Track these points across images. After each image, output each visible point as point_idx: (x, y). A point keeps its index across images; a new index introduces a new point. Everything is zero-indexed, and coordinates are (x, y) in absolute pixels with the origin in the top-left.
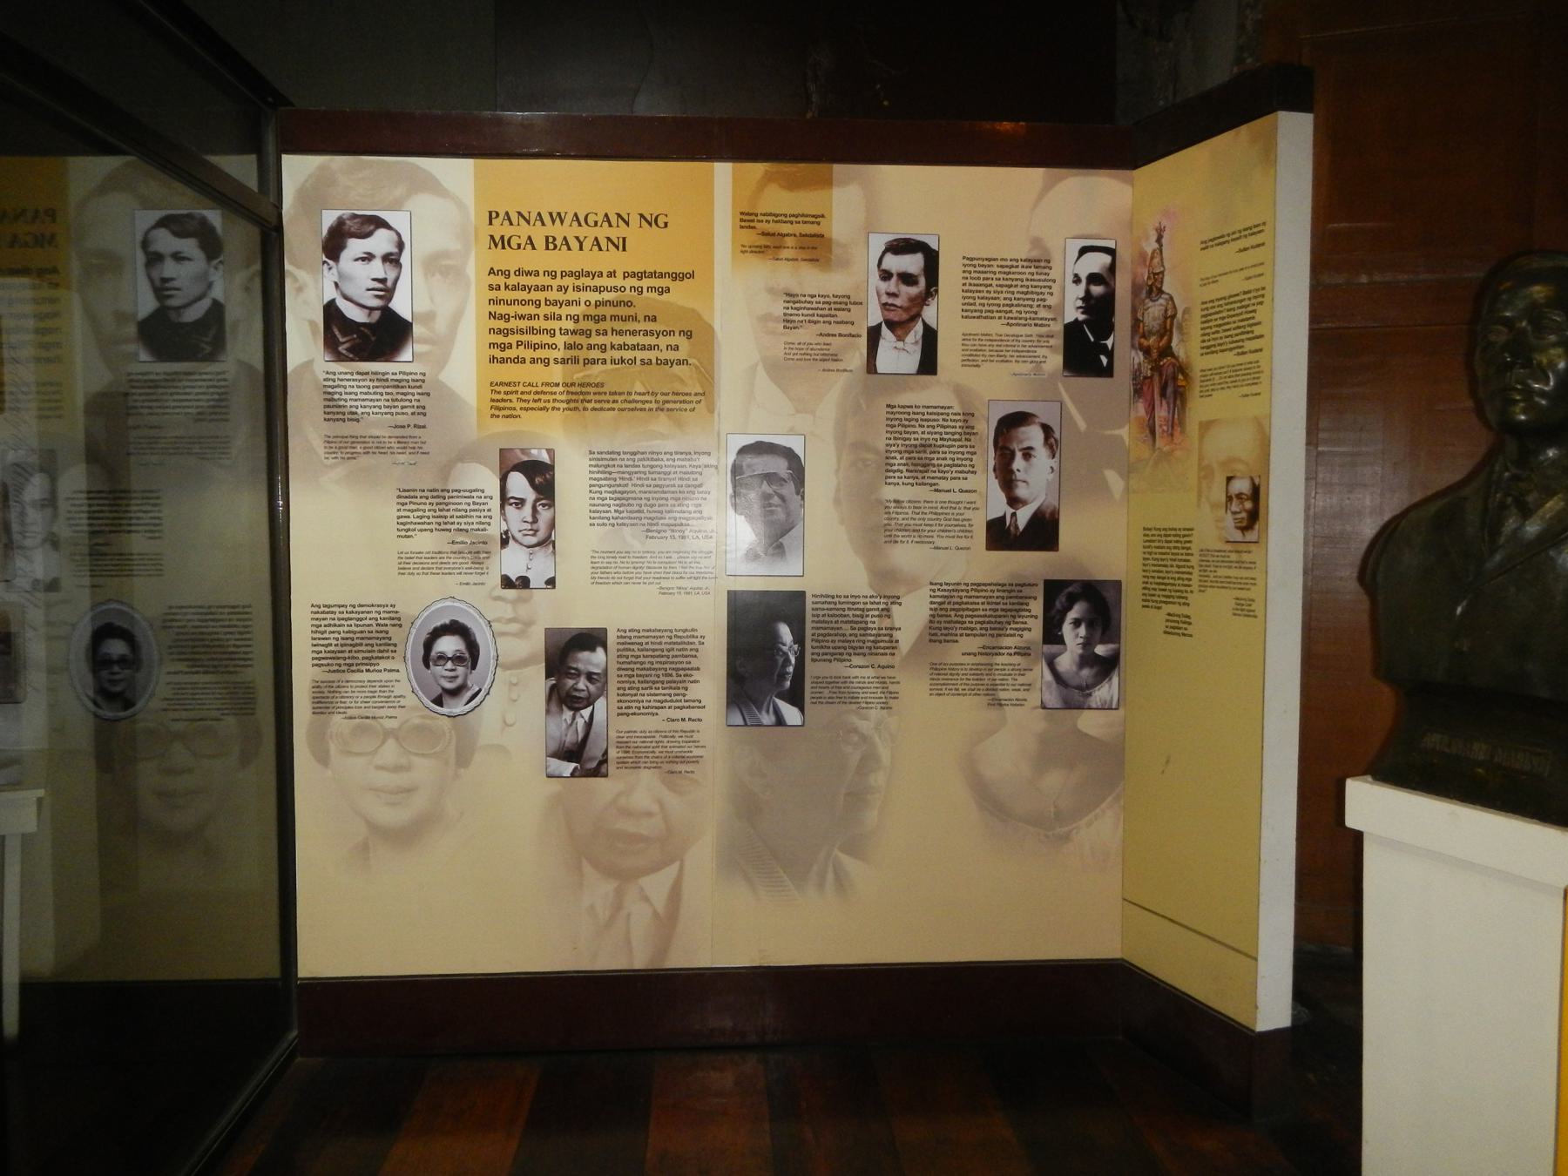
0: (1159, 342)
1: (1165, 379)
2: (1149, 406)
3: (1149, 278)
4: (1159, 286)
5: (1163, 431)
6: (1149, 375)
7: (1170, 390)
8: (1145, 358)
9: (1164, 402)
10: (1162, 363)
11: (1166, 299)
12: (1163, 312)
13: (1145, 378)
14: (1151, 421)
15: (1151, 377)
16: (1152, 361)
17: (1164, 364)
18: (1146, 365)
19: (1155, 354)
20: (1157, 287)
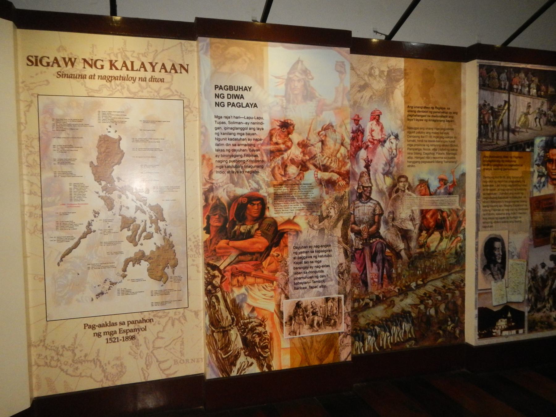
0: (368, 230)
1: (375, 251)
2: (361, 267)
3: (357, 189)
4: (368, 195)
5: (374, 282)
6: (360, 248)
7: (379, 257)
8: (357, 237)
9: (374, 265)
10: (371, 241)
11: (374, 204)
12: (371, 211)
13: (356, 249)
14: (363, 276)
15: (363, 250)
16: (363, 240)
17: (374, 242)
18: (357, 241)
19: (365, 235)
20: (366, 195)
